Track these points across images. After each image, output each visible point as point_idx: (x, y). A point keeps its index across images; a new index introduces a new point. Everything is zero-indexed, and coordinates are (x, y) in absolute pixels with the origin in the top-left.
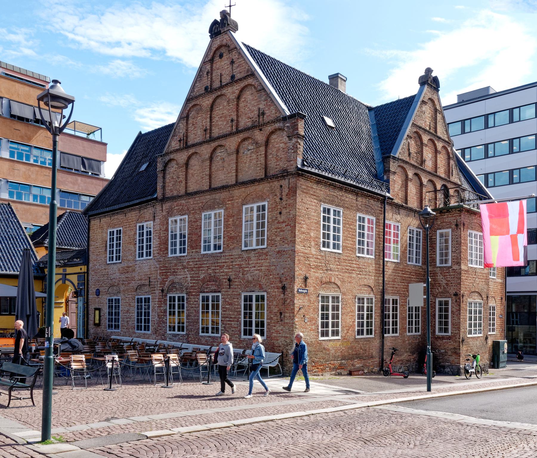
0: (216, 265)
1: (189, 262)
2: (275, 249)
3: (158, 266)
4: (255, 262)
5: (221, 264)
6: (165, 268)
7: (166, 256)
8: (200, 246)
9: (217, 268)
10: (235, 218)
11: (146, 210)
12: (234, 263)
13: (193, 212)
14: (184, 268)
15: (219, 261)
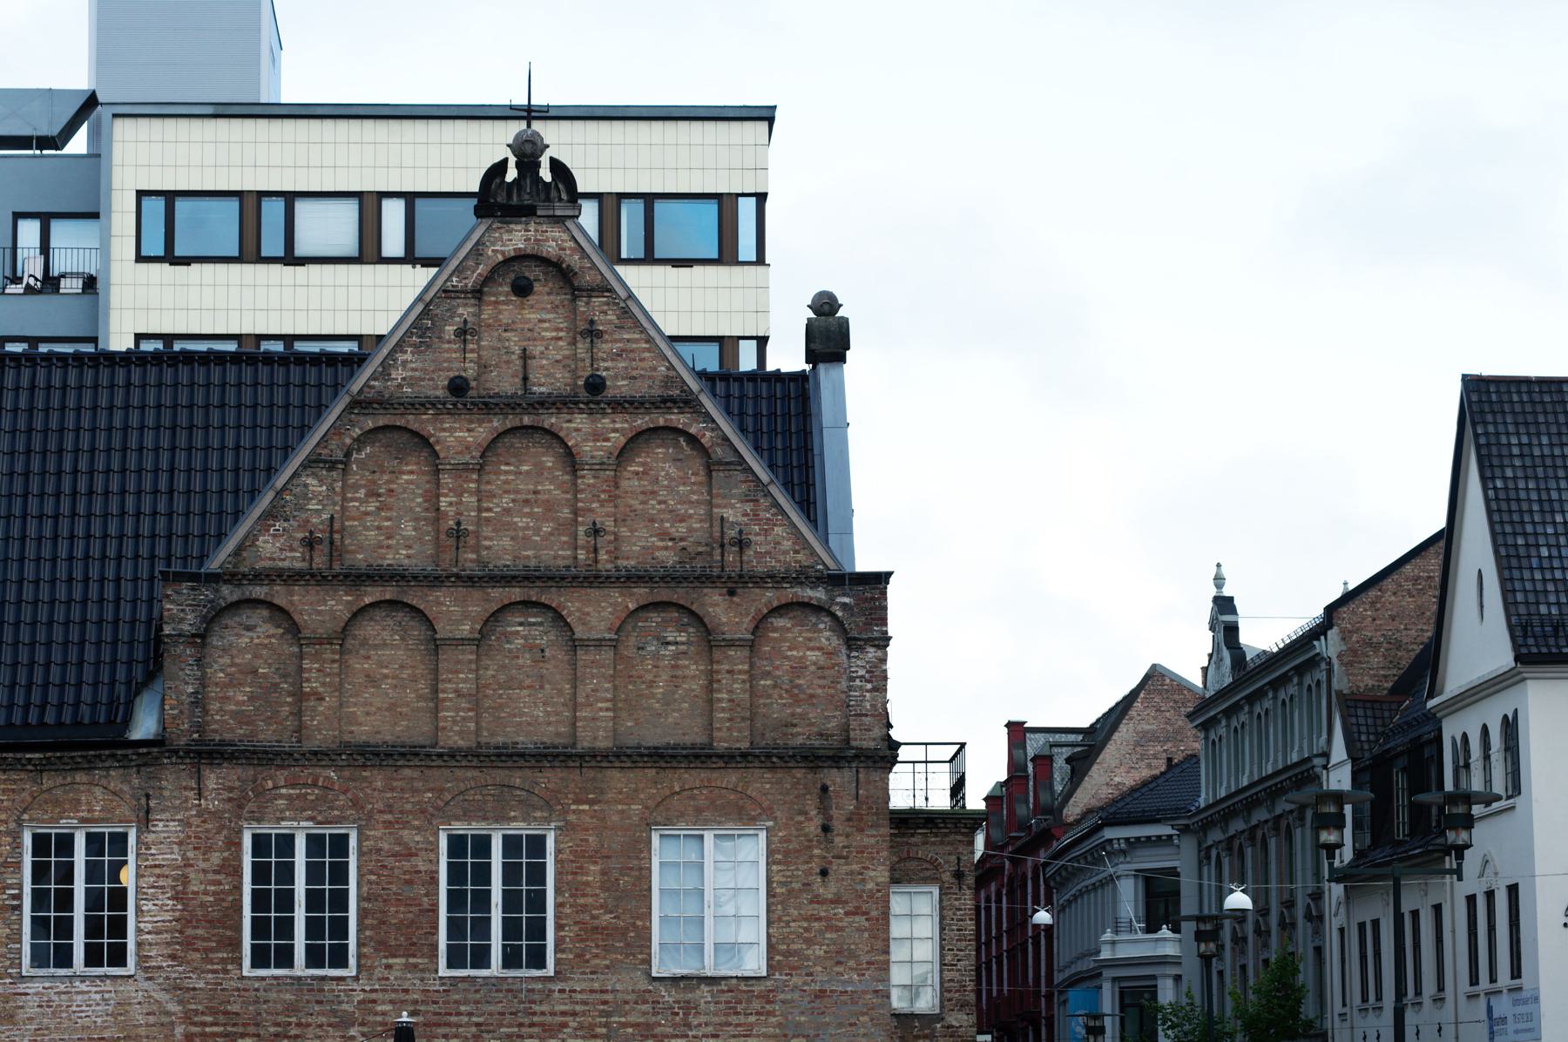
0: (526, 1021)
1: (374, 1001)
2: (805, 983)
3: (173, 1007)
4: (716, 1019)
5: (548, 1019)
6: (221, 1018)
7: (226, 971)
8: (435, 947)
9: (525, 1030)
10: (614, 864)
11: (80, 777)
12: (613, 1019)
13: (388, 817)
14: (345, 1022)
15: (536, 1008)
